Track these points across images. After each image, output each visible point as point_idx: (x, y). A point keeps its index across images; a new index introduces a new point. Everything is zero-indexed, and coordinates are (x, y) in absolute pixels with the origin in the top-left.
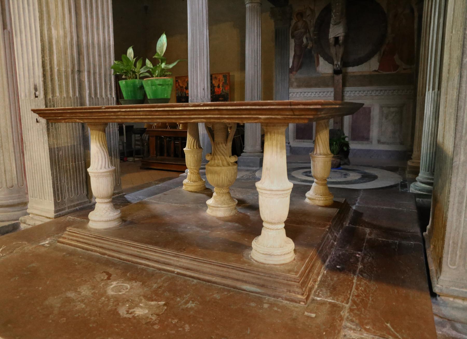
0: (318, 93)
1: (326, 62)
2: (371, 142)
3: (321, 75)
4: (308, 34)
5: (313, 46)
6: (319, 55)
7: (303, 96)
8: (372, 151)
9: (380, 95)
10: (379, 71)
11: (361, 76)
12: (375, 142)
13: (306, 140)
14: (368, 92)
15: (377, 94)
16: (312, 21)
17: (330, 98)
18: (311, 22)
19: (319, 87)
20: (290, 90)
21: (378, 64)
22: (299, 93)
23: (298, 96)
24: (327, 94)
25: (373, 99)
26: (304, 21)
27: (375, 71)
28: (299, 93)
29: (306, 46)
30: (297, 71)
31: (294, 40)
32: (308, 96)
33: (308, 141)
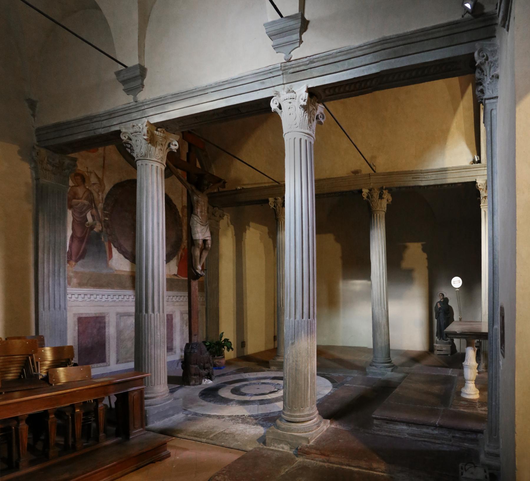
4: (94, 210)
16: (100, 193)
18: (99, 195)
20: (68, 289)
22: (83, 296)
29: (92, 228)
32: (96, 300)
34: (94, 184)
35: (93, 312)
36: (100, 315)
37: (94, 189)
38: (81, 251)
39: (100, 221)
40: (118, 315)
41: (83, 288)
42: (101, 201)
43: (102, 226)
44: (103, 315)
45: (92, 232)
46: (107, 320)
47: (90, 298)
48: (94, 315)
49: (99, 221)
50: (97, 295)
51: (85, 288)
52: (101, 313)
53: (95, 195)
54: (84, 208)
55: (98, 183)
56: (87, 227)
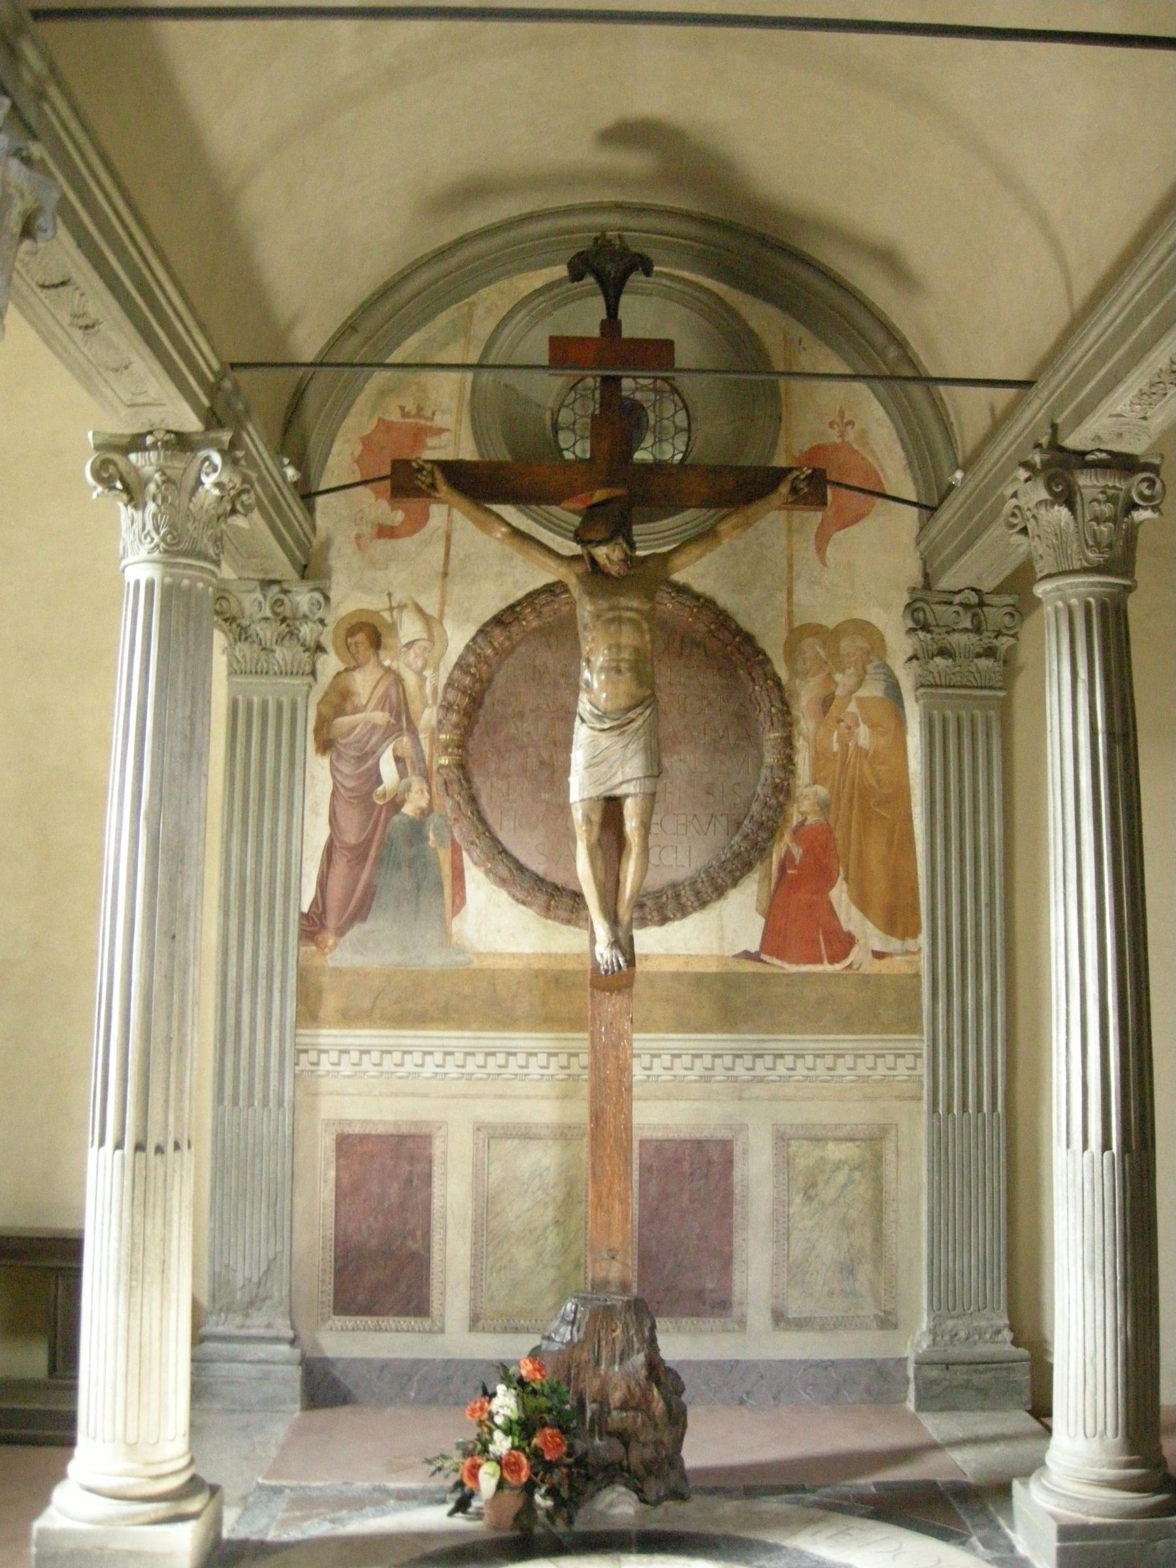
0: (459, 1058)
1: (502, 896)
2: (742, 1323)
3: (476, 964)
4: (405, 739)
5: (430, 802)
6: (465, 855)
7: (373, 1071)
8: (751, 1366)
9: (772, 1075)
10: (764, 957)
11: (677, 976)
12: (758, 1316)
13: (391, 1321)
14: (718, 1061)
15: (760, 1071)
16: (428, 673)
17: (521, 1084)
18: (422, 679)
19: (462, 1025)
21: (758, 924)
23: (346, 1069)
24: (505, 1067)
25: (740, 1098)
26: (388, 670)
27: (747, 955)
28: (355, 1055)
29: (395, 805)
30: (341, 932)
32: (401, 1072)
33: (404, 1322)
34: (410, 645)
35: (389, 1117)
36: (413, 1131)
37: (407, 667)
38: (357, 895)
39: (426, 776)
40: (481, 1135)
41: (356, 1028)
42: (430, 702)
43: (430, 792)
44: (424, 1130)
45: (396, 819)
46: (437, 1149)
47: (380, 1065)
48: (391, 1130)
49: (421, 775)
50: (405, 1052)
51: (364, 1027)
52: (416, 1123)
53: (411, 680)
54: (374, 739)
55: (425, 636)
56: (380, 803)
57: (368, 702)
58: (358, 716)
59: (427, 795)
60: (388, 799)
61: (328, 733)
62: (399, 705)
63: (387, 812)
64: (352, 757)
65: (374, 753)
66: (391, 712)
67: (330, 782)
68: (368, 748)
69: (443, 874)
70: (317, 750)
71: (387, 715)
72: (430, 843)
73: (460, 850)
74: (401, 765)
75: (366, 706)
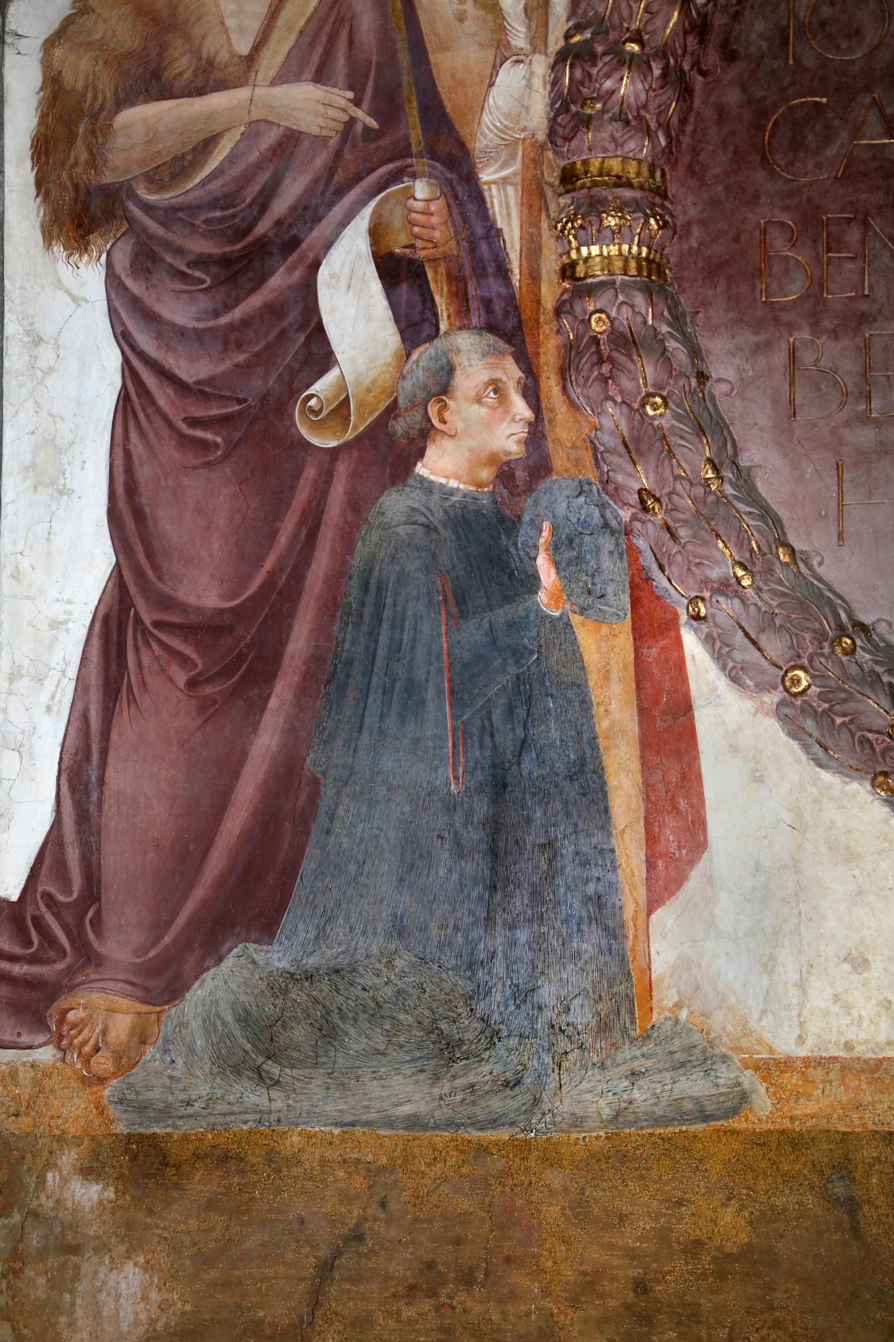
4: (421, 189)
31: (112, 280)
42: (519, 37)
49: (491, 328)
57: (257, 48)
58: (217, 100)
59: (521, 408)
60: (357, 425)
61: (95, 160)
62: (389, 60)
63: (354, 476)
64: (201, 262)
65: (293, 244)
66: (355, 85)
67: (112, 357)
68: (263, 227)
69: (603, 725)
70: (48, 237)
71: (341, 97)
72: (542, 597)
73: (671, 625)
74: (404, 290)
75: (251, 59)
